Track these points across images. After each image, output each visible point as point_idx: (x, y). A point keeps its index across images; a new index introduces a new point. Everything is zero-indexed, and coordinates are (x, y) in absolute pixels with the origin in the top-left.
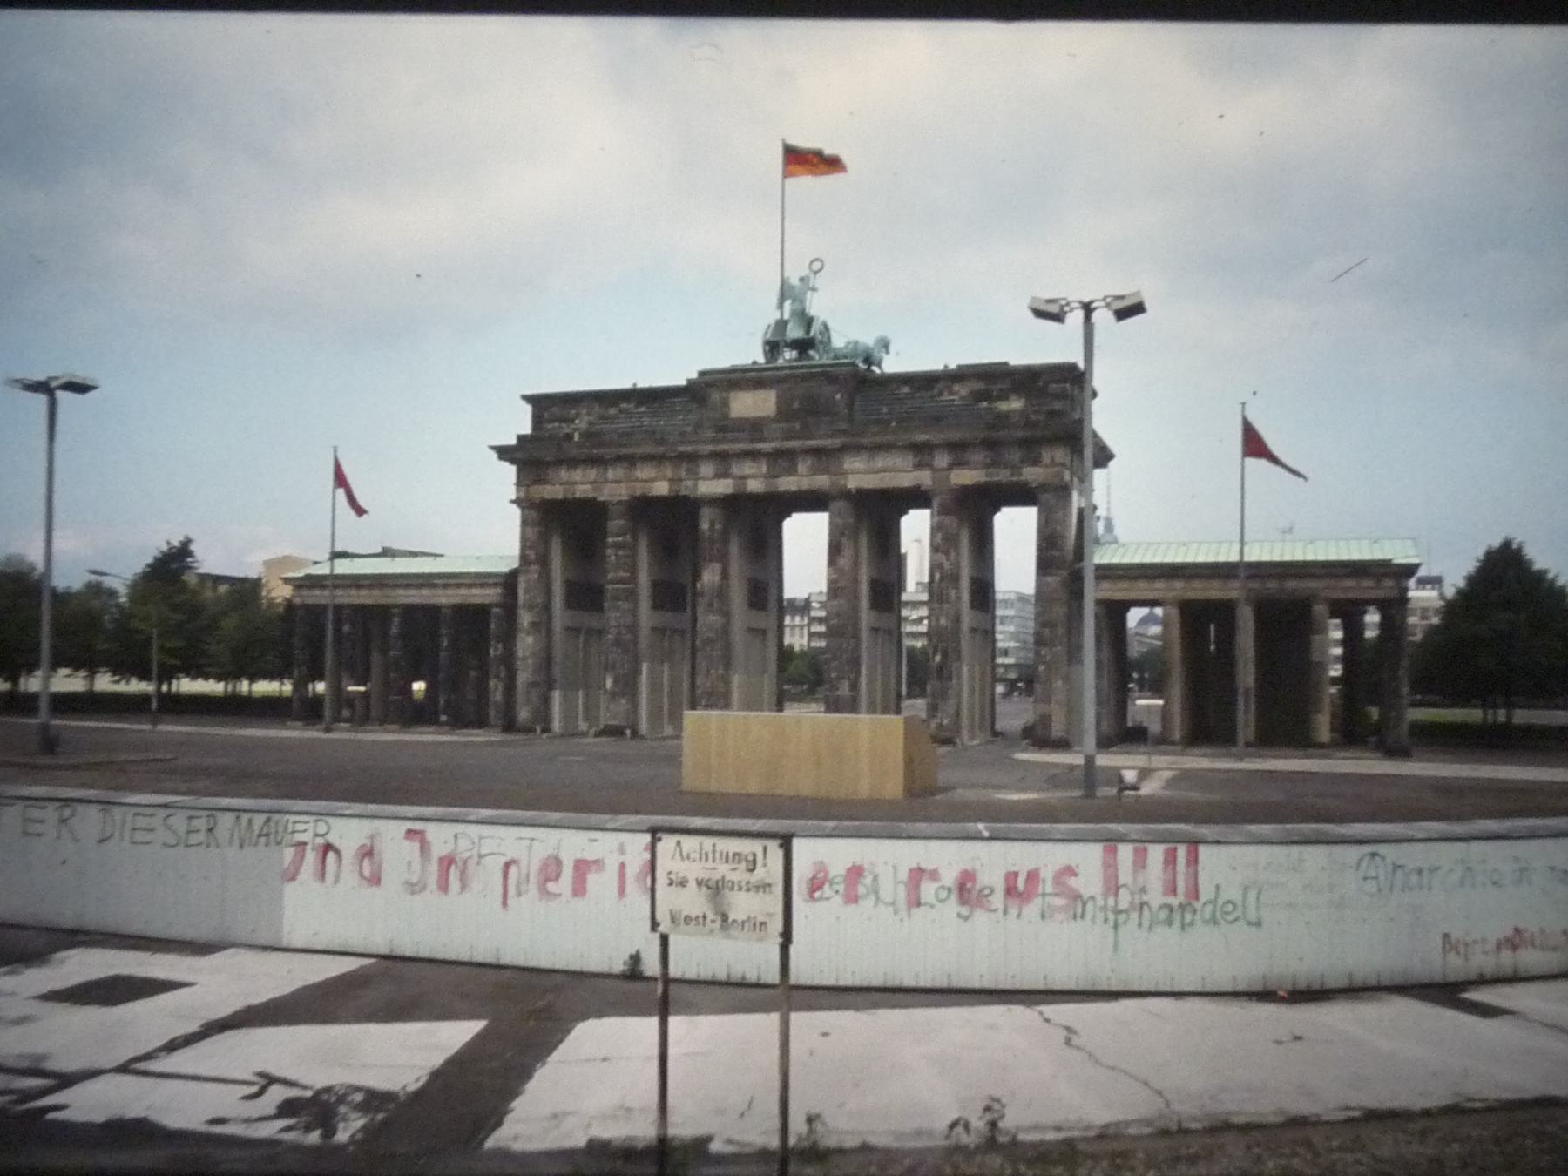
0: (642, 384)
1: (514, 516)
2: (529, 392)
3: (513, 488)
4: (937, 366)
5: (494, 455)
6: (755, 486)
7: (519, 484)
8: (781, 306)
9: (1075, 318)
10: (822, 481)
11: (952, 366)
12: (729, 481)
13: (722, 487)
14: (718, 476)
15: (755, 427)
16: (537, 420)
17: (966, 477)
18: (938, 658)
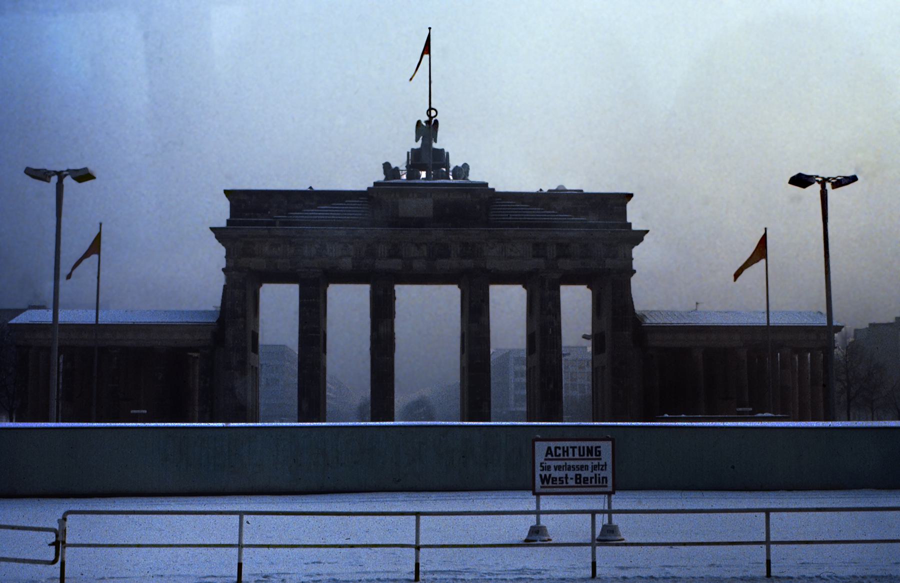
0: (317, 187)
1: (220, 280)
2: (230, 187)
3: (224, 260)
4: (533, 188)
5: (213, 235)
6: (419, 265)
7: (227, 257)
8: (417, 140)
9: (816, 188)
10: (468, 263)
11: (545, 190)
12: (399, 261)
13: (395, 264)
14: (391, 257)
15: (420, 223)
16: (235, 210)
17: (566, 265)
18: (551, 386)
